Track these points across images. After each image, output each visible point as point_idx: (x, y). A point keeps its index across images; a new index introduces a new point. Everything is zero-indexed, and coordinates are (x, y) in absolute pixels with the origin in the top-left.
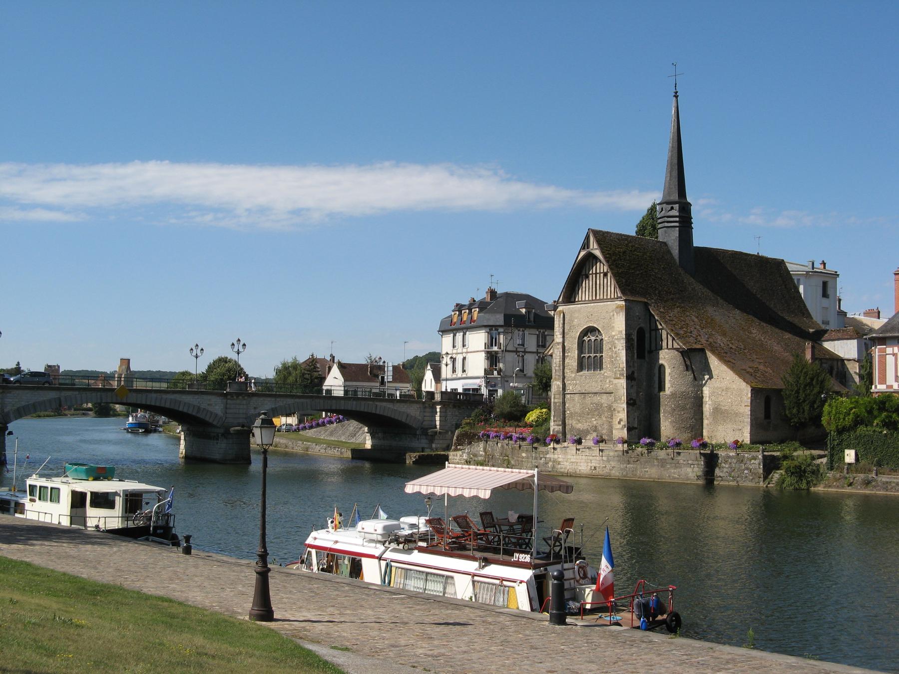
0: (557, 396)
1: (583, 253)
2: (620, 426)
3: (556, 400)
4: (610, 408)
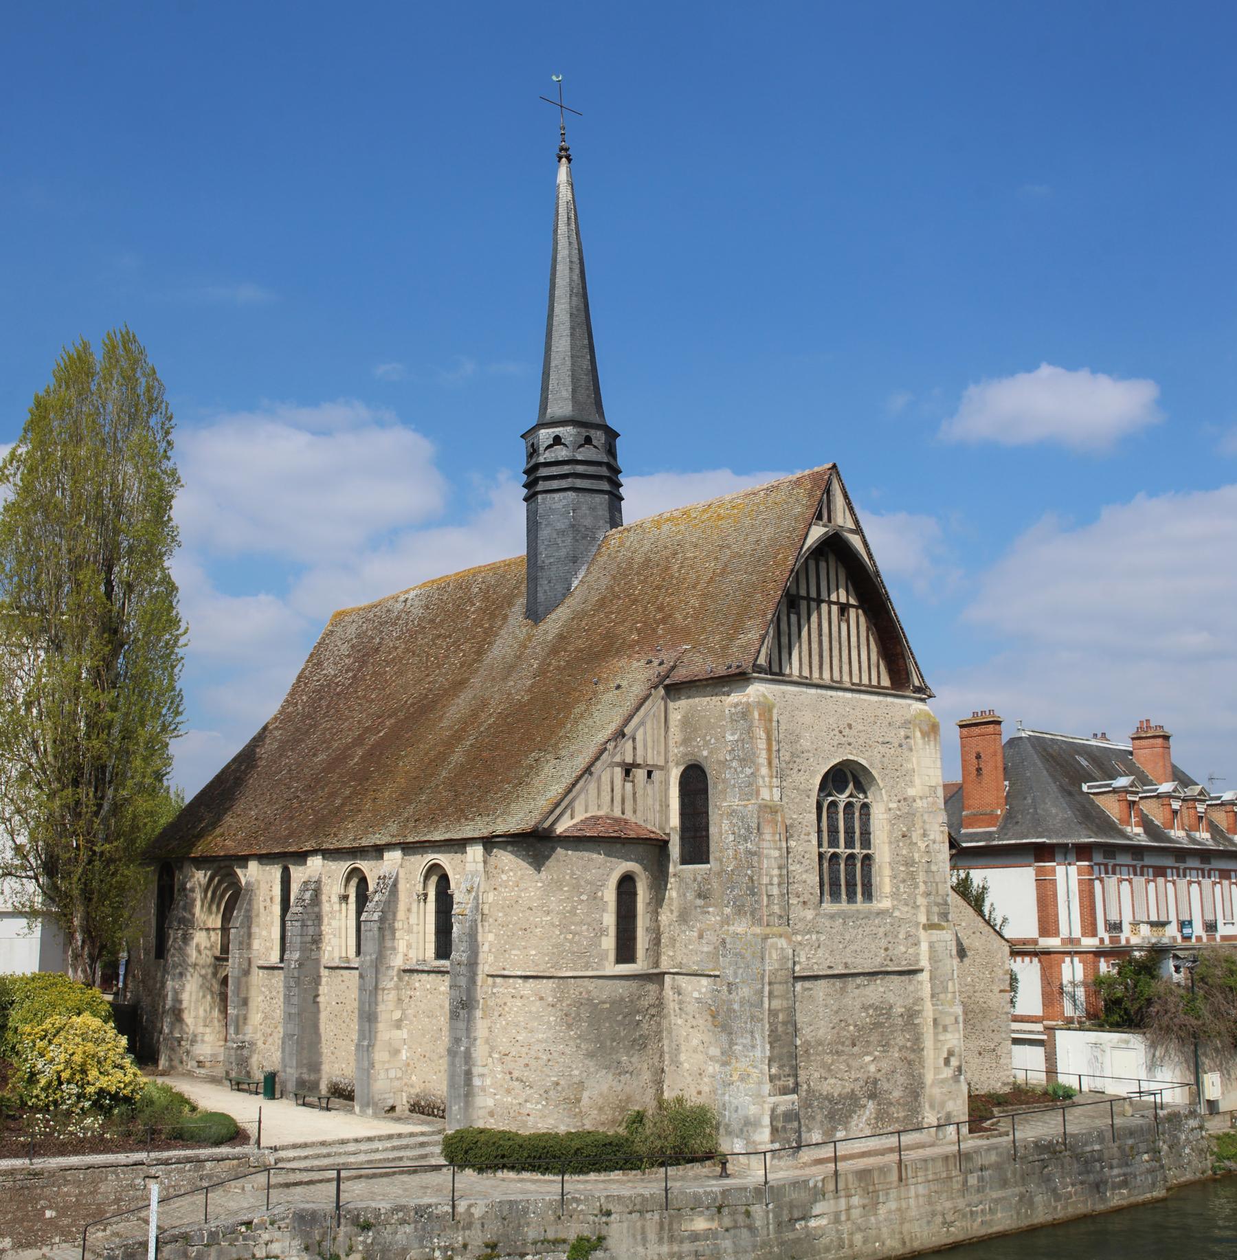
0: (779, 989)
1: (817, 533)
2: (948, 1073)
3: (776, 1004)
4: (911, 1015)
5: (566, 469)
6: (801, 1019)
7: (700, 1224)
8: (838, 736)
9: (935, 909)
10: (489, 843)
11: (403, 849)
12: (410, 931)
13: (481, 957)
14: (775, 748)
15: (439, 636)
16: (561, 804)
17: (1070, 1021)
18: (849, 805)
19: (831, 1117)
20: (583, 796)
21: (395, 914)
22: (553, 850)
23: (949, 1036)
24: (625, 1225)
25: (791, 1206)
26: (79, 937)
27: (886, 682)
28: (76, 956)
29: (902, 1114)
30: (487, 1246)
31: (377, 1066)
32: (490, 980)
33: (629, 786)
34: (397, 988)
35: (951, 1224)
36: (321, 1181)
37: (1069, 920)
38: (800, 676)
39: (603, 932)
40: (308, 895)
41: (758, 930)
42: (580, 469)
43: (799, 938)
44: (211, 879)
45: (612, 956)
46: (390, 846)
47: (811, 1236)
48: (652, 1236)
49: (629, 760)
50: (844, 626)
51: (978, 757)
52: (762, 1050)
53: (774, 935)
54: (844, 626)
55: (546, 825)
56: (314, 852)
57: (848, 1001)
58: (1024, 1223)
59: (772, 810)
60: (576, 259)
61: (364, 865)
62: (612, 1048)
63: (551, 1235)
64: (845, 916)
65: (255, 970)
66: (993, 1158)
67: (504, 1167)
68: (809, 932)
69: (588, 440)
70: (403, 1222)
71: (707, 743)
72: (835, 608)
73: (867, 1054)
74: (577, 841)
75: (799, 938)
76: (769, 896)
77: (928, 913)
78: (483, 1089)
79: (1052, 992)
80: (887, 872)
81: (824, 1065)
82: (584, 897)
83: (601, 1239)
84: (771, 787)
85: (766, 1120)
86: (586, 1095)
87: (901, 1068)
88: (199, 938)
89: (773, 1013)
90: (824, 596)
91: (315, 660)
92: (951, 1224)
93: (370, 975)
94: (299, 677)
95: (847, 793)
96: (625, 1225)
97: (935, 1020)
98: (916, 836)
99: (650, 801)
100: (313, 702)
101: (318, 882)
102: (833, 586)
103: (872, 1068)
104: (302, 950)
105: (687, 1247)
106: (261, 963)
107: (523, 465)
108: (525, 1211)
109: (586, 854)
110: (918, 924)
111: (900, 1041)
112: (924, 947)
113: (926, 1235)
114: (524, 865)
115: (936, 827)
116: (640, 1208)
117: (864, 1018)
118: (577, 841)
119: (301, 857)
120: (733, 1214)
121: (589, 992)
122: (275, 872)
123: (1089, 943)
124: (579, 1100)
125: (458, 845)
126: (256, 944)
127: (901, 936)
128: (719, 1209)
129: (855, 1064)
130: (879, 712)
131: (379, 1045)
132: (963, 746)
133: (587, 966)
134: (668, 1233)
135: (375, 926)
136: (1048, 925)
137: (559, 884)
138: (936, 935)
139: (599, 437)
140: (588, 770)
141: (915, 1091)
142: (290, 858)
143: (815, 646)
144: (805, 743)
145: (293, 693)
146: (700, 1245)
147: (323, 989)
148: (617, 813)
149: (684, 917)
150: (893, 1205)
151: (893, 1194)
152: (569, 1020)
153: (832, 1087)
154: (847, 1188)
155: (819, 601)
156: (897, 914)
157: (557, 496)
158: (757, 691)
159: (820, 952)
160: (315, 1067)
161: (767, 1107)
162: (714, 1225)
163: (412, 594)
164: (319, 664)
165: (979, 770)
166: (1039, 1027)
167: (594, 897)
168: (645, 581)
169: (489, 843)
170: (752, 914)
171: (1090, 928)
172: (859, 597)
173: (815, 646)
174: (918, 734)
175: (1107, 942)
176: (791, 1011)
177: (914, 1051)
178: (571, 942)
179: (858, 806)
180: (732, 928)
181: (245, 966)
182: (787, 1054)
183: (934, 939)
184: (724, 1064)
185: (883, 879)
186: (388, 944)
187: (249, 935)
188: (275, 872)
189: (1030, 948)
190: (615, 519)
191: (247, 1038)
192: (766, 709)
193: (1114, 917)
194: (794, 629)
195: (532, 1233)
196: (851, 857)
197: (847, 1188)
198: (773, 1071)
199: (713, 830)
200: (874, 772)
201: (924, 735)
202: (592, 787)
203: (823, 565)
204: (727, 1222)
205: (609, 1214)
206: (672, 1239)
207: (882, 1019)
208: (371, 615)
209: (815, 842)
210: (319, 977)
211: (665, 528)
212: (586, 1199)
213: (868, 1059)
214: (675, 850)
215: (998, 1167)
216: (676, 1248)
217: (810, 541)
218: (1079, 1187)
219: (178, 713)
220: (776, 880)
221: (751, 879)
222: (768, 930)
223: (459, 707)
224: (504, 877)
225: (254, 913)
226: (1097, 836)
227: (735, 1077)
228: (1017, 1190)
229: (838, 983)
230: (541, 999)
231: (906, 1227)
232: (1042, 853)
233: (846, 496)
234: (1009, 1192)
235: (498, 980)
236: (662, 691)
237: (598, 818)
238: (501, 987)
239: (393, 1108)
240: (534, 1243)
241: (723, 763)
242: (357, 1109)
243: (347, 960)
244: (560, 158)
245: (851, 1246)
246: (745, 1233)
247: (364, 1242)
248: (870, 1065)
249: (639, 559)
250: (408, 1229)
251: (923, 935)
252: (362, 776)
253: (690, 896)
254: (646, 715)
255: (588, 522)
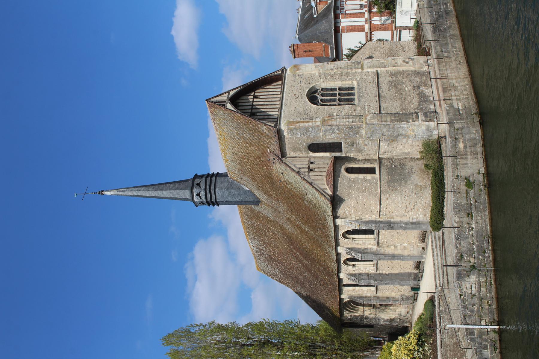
0: (384, 119)
1: (229, 106)
2: (411, 62)
3: (389, 120)
4: (392, 74)
5: (208, 192)
6: (394, 111)
7: (461, 145)
8: (299, 99)
9: (356, 66)
10: (335, 217)
11: (337, 246)
12: (365, 244)
13: (373, 219)
14: (303, 120)
15: (265, 235)
16: (322, 192)
17: (393, 22)
18: (322, 95)
19: (426, 102)
20: (319, 185)
21: (359, 249)
22: (337, 195)
23: (399, 62)
24: (461, 170)
25: (455, 115)
26: (366, 353)
27: (280, 83)
28: (372, 354)
29: (425, 78)
30: (468, 216)
31: (409, 254)
32: (381, 216)
33: (316, 170)
34: (384, 247)
35: (460, 62)
36: (447, 272)
37: (359, 21)
38: (278, 112)
39: (365, 178)
40: (353, 278)
41: (364, 126)
42: (208, 187)
43: (367, 112)
44: (347, 310)
45: (373, 175)
46: (336, 251)
47: (465, 108)
48: (465, 161)
49: (307, 170)
50: (261, 97)
51: (305, 52)
52: (404, 124)
53: (366, 120)
54: (261, 97)
55: (329, 198)
56: (338, 276)
57: (387, 96)
58: (459, 38)
59: (324, 121)
60: (136, 189)
61: (343, 259)
62: (404, 175)
63: (465, 195)
64: (359, 97)
65: (378, 295)
66: (438, 48)
67: (442, 211)
68: (365, 109)
69: (198, 184)
70: (460, 244)
71: (301, 143)
72: (255, 100)
73: (405, 89)
74: (335, 187)
75: (367, 112)
76: (353, 122)
77: (358, 68)
78: (417, 218)
79: (383, 27)
80: (344, 82)
81: (409, 103)
82: (353, 185)
83: (466, 178)
84: (316, 121)
85: (427, 123)
86: (419, 184)
87: (409, 78)
88: (367, 314)
89: (392, 121)
90: (251, 104)
91: (273, 276)
92: (460, 62)
93: (379, 257)
94: (279, 282)
95: (318, 96)
96: (461, 170)
97: (393, 67)
98: (332, 73)
99: (321, 163)
100: (288, 277)
101: (348, 274)
102: (247, 101)
103: (410, 88)
104: (371, 279)
105: (468, 150)
106: (375, 293)
107: (207, 206)
108: (457, 204)
109: (339, 184)
110: (362, 72)
111: (400, 78)
112: (369, 70)
113: (463, 70)
114: (342, 205)
115: (329, 66)
116: (456, 165)
117: (393, 90)
118: (335, 187)
119: (340, 280)
120: (458, 134)
121: (385, 183)
122: (345, 289)
123: (367, 15)
124: (421, 186)
125: (336, 227)
126: (369, 295)
127: (366, 78)
128: (456, 139)
129: (408, 94)
130: (290, 85)
131: (402, 253)
132: (302, 57)
133: (377, 184)
134: (464, 156)
135: (363, 255)
136: (361, 29)
137: (349, 193)
138: (365, 66)
139: (197, 181)
140: (311, 184)
141: (417, 73)
142: (340, 284)
143: (268, 107)
144: (301, 110)
145: (285, 284)
146: (468, 145)
147: (384, 272)
148: (325, 174)
149: (360, 151)
150: (454, 81)
151: (450, 81)
152: (394, 190)
153: (416, 101)
154: (449, 96)
155: (253, 105)
156: (358, 79)
157: (217, 195)
158: (283, 126)
159: (371, 105)
160: (409, 274)
161: (423, 123)
162: (461, 141)
163: (251, 244)
164: (275, 275)
165: (309, 51)
166: (395, 32)
167: (353, 181)
168: (246, 165)
169: (335, 217)
170: (359, 128)
171: (362, 15)
172: (251, 92)
173: (268, 107)
174: (298, 72)
175: (366, 9)
176: (391, 115)
177: (404, 74)
178: (368, 189)
179: (322, 92)
180: (364, 135)
181: (376, 298)
182: (405, 116)
183: (366, 67)
184: (409, 137)
185: (347, 83)
186: (369, 251)
187: (366, 297)
188: (345, 289)
189: (369, 35)
190: (225, 175)
191: (400, 297)
192: (289, 123)
193: (358, 7)
194: (262, 114)
195: (464, 202)
196: (339, 94)
197: (449, 96)
198: (411, 121)
199: (331, 141)
200: (311, 87)
201: (298, 70)
202: (316, 182)
203: (240, 104)
204: (460, 136)
205: (458, 176)
206: (466, 155)
207: (393, 84)
208: (258, 258)
209: (334, 107)
210: (380, 274)
211: (228, 158)
212: (453, 183)
213: (406, 89)
214: (337, 154)
215: (441, 46)
216: (469, 153)
217: (232, 108)
218: (447, 19)
219: (292, 322)
220: (347, 120)
221: (347, 128)
222: (364, 123)
223: (289, 228)
224: (347, 212)
225: (359, 296)
226: (331, 12)
227: (413, 134)
228: (449, 40)
229: (382, 99)
230: (387, 199)
231: (461, 77)
232: (337, 30)
233: (217, 96)
234: (449, 42)
235: (381, 213)
236: (284, 159)
237: (327, 180)
238: (383, 212)
239: (423, 248)
240: (467, 200)
241: (308, 138)
242: (423, 260)
243: (374, 264)
244: (102, 194)
245: (468, 95)
246: (464, 130)
247: (467, 257)
248: (408, 88)
249: (238, 167)
250: (463, 243)
251: (365, 70)
252: (313, 260)
253: (353, 149)
254: (292, 164)
255: (226, 184)
